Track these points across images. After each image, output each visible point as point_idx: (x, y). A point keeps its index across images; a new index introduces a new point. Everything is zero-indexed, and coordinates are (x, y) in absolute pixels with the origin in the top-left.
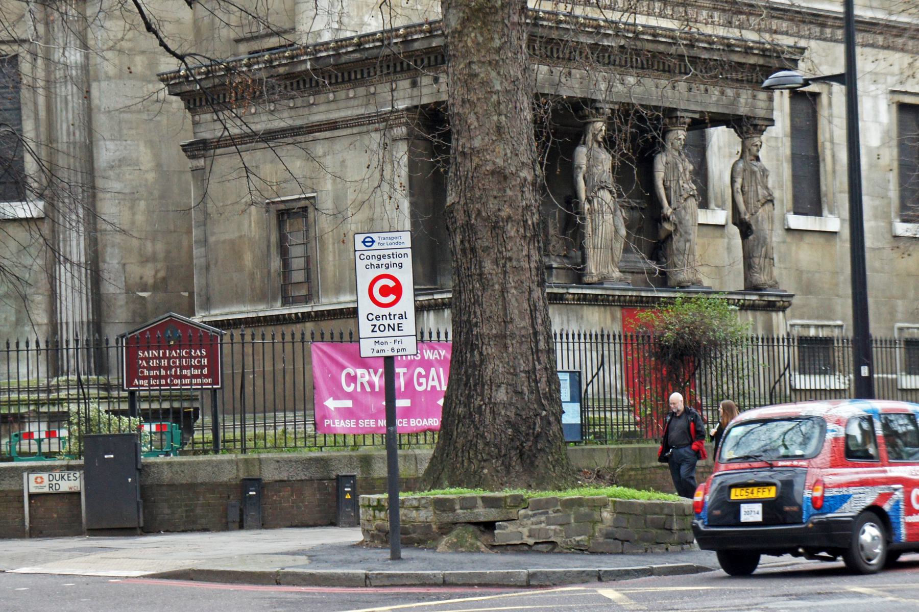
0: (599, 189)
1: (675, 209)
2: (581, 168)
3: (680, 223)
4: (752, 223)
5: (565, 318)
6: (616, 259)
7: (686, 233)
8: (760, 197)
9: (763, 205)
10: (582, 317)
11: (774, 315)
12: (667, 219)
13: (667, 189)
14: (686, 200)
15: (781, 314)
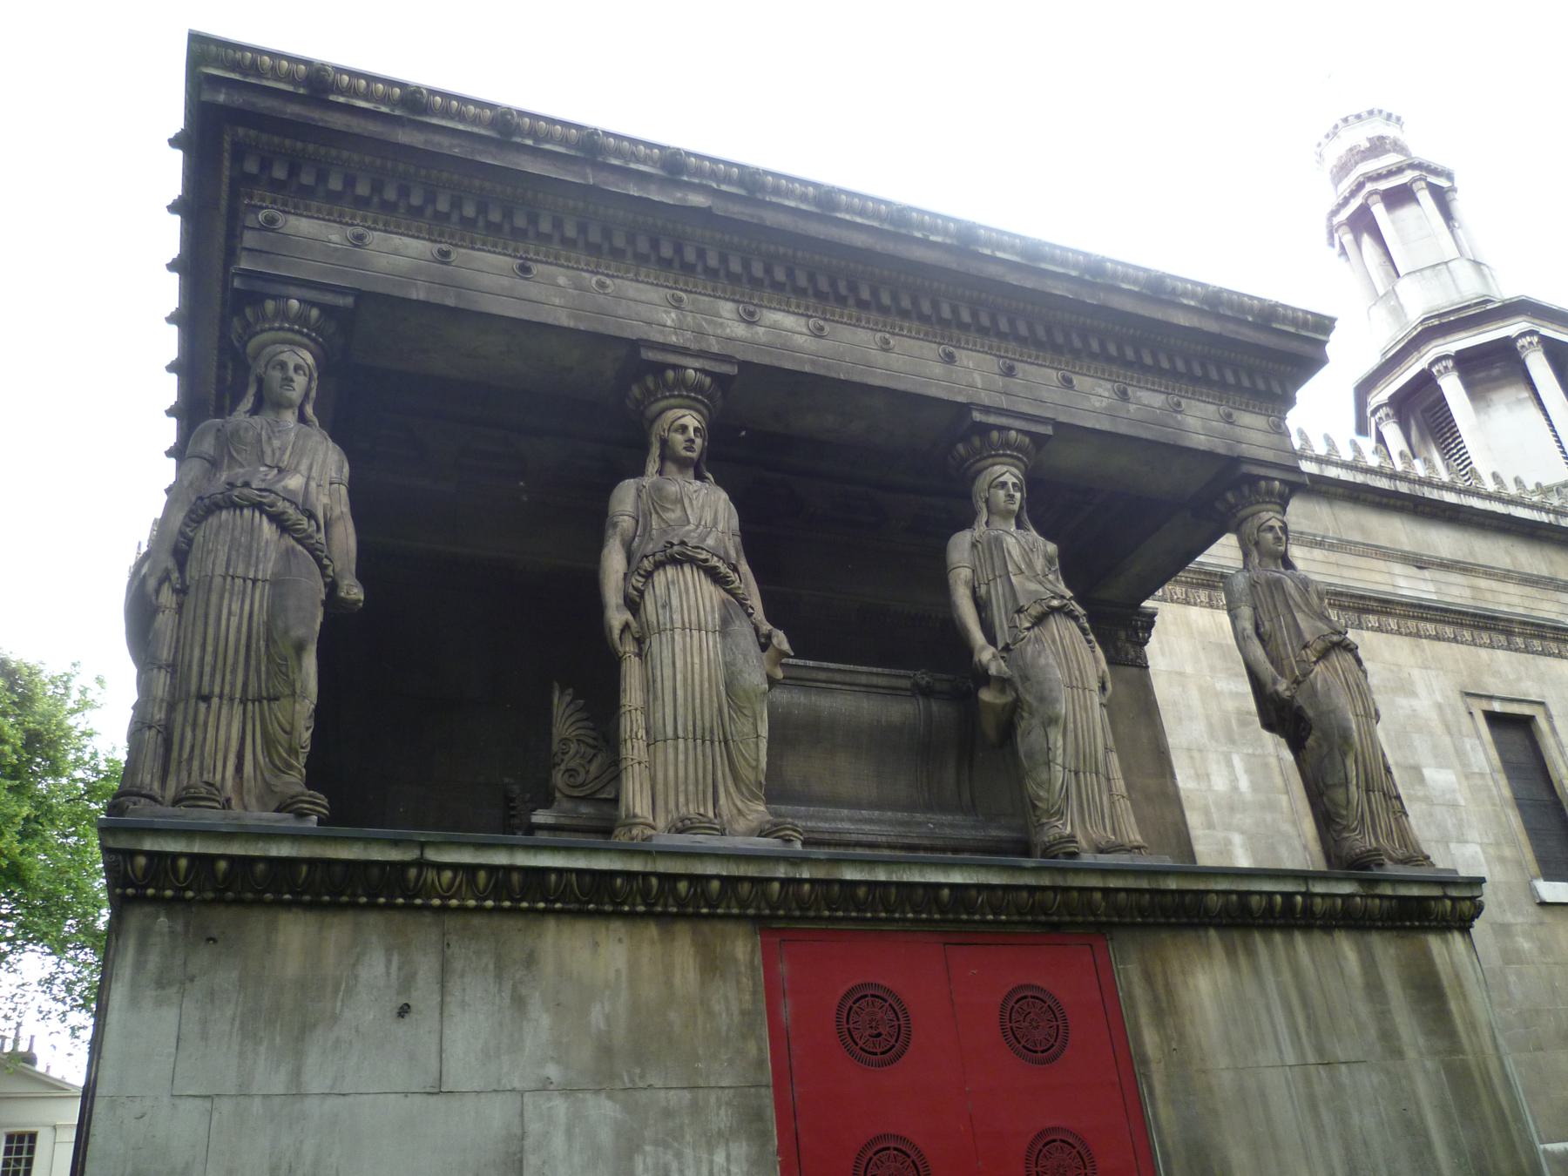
0: (660, 565)
1: (1007, 648)
2: (615, 525)
3: (1025, 678)
4: (1300, 700)
5: (426, 967)
6: (746, 773)
7: (1042, 699)
8: (1308, 637)
9: (1324, 655)
10: (531, 960)
11: (1434, 942)
12: (982, 677)
13: (981, 605)
14: (1040, 620)
15: (1457, 939)
